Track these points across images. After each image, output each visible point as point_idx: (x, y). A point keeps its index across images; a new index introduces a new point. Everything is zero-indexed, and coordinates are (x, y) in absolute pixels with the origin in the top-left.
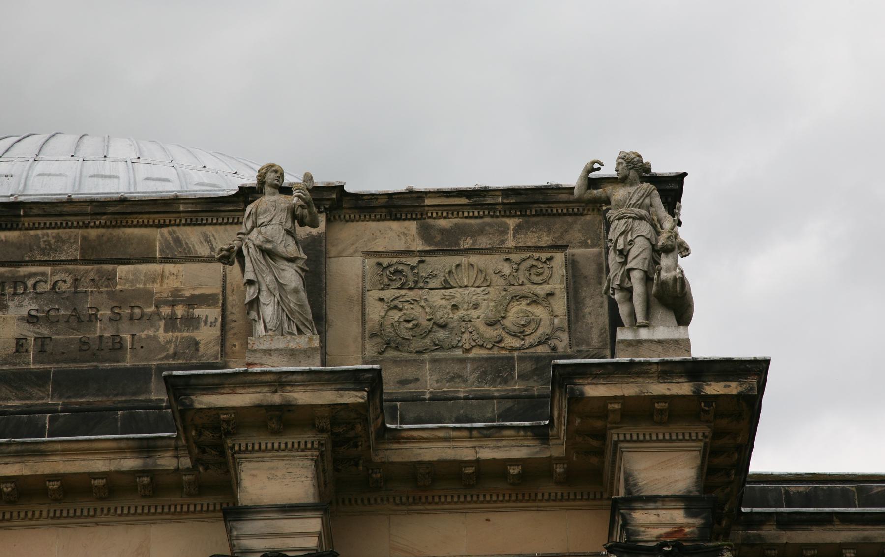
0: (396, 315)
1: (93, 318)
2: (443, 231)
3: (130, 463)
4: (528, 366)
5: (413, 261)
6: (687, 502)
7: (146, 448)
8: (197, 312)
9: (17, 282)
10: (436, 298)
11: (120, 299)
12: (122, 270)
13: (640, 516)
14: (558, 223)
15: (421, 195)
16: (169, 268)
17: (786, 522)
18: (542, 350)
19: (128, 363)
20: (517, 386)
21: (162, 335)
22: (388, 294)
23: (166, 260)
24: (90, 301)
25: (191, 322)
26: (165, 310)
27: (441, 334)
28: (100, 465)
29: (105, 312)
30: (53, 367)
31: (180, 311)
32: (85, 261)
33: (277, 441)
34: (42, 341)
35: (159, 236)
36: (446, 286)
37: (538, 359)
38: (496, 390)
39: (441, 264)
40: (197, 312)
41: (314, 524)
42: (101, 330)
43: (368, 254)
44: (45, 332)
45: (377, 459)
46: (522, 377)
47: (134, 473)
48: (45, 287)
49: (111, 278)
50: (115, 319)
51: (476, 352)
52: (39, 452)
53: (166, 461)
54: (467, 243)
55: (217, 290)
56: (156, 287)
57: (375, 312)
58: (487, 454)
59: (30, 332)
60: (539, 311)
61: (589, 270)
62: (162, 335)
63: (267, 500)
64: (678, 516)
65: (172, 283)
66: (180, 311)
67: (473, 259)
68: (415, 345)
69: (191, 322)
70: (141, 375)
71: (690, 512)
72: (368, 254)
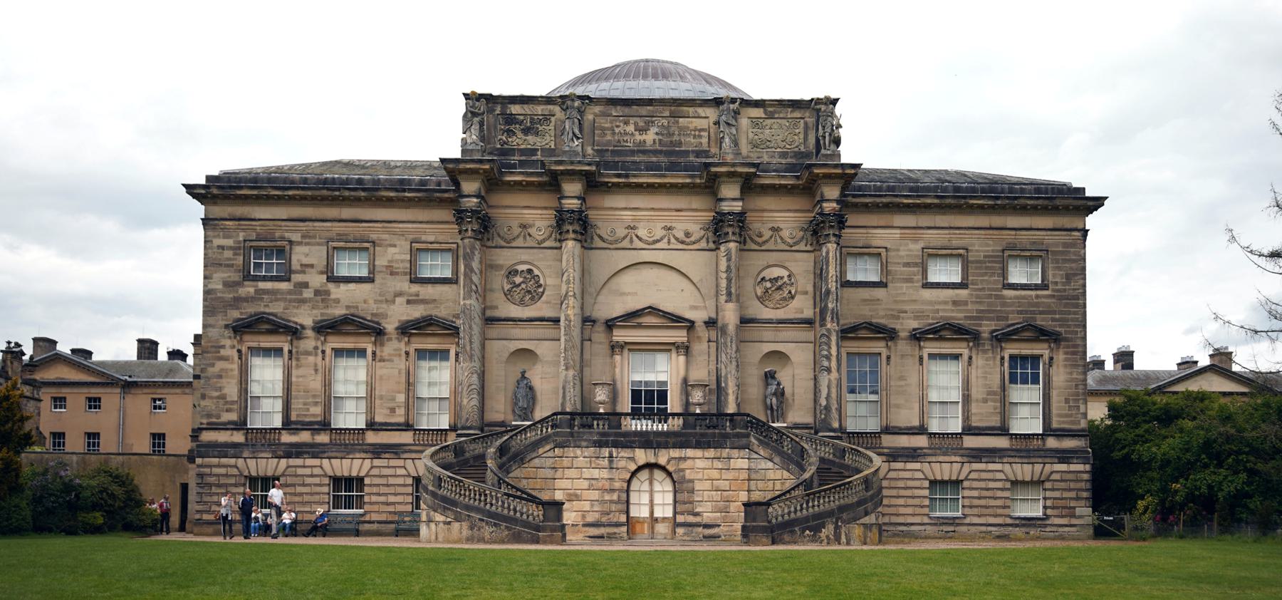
0: (756, 137)
1: (673, 134)
2: (770, 112)
3: (688, 181)
4: (792, 154)
5: (761, 121)
6: (838, 202)
7: (692, 177)
8: (702, 133)
9: (653, 122)
10: (767, 131)
11: (680, 129)
12: (681, 120)
13: (825, 205)
14: (802, 111)
15: (764, 101)
16: (694, 120)
17: (854, 196)
18: (797, 149)
19: (683, 149)
20: (789, 160)
21: (692, 141)
22: (754, 130)
23: (692, 117)
24: (673, 129)
25: (700, 137)
26: (693, 133)
27: (768, 143)
28: (680, 181)
29: (676, 133)
30: (664, 149)
31: (697, 133)
32: (670, 117)
33: (731, 180)
34: (660, 140)
35: (691, 110)
36: (771, 128)
37: (795, 152)
38: (784, 161)
39: (769, 122)
40: (702, 133)
41: (740, 204)
42: (676, 138)
43: (749, 118)
44: (661, 137)
45: (754, 182)
46: (791, 157)
47: (689, 183)
48: (660, 124)
49: (678, 122)
50: (679, 135)
51: (778, 150)
52: (664, 176)
53: (698, 181)
54: (776, 116)
55: (707, 127)
56: (690, 125)
57: (751, 135)
58: (783, 182)
59: (657, 138)
60: (796, 137)
61: (810, 125)
62: (692, 141)
63: (728, 196)
64: (835, 205)
65: (694, 125)
66: (697, 133)
67: (778, 121)
68: (762, 147)
69: (700, 137)
70: (687, 152)
71: (838, 204)
72: (749, 118)
